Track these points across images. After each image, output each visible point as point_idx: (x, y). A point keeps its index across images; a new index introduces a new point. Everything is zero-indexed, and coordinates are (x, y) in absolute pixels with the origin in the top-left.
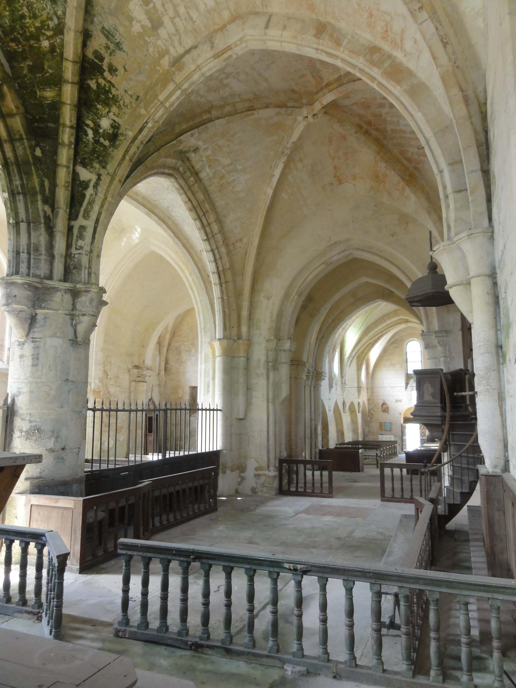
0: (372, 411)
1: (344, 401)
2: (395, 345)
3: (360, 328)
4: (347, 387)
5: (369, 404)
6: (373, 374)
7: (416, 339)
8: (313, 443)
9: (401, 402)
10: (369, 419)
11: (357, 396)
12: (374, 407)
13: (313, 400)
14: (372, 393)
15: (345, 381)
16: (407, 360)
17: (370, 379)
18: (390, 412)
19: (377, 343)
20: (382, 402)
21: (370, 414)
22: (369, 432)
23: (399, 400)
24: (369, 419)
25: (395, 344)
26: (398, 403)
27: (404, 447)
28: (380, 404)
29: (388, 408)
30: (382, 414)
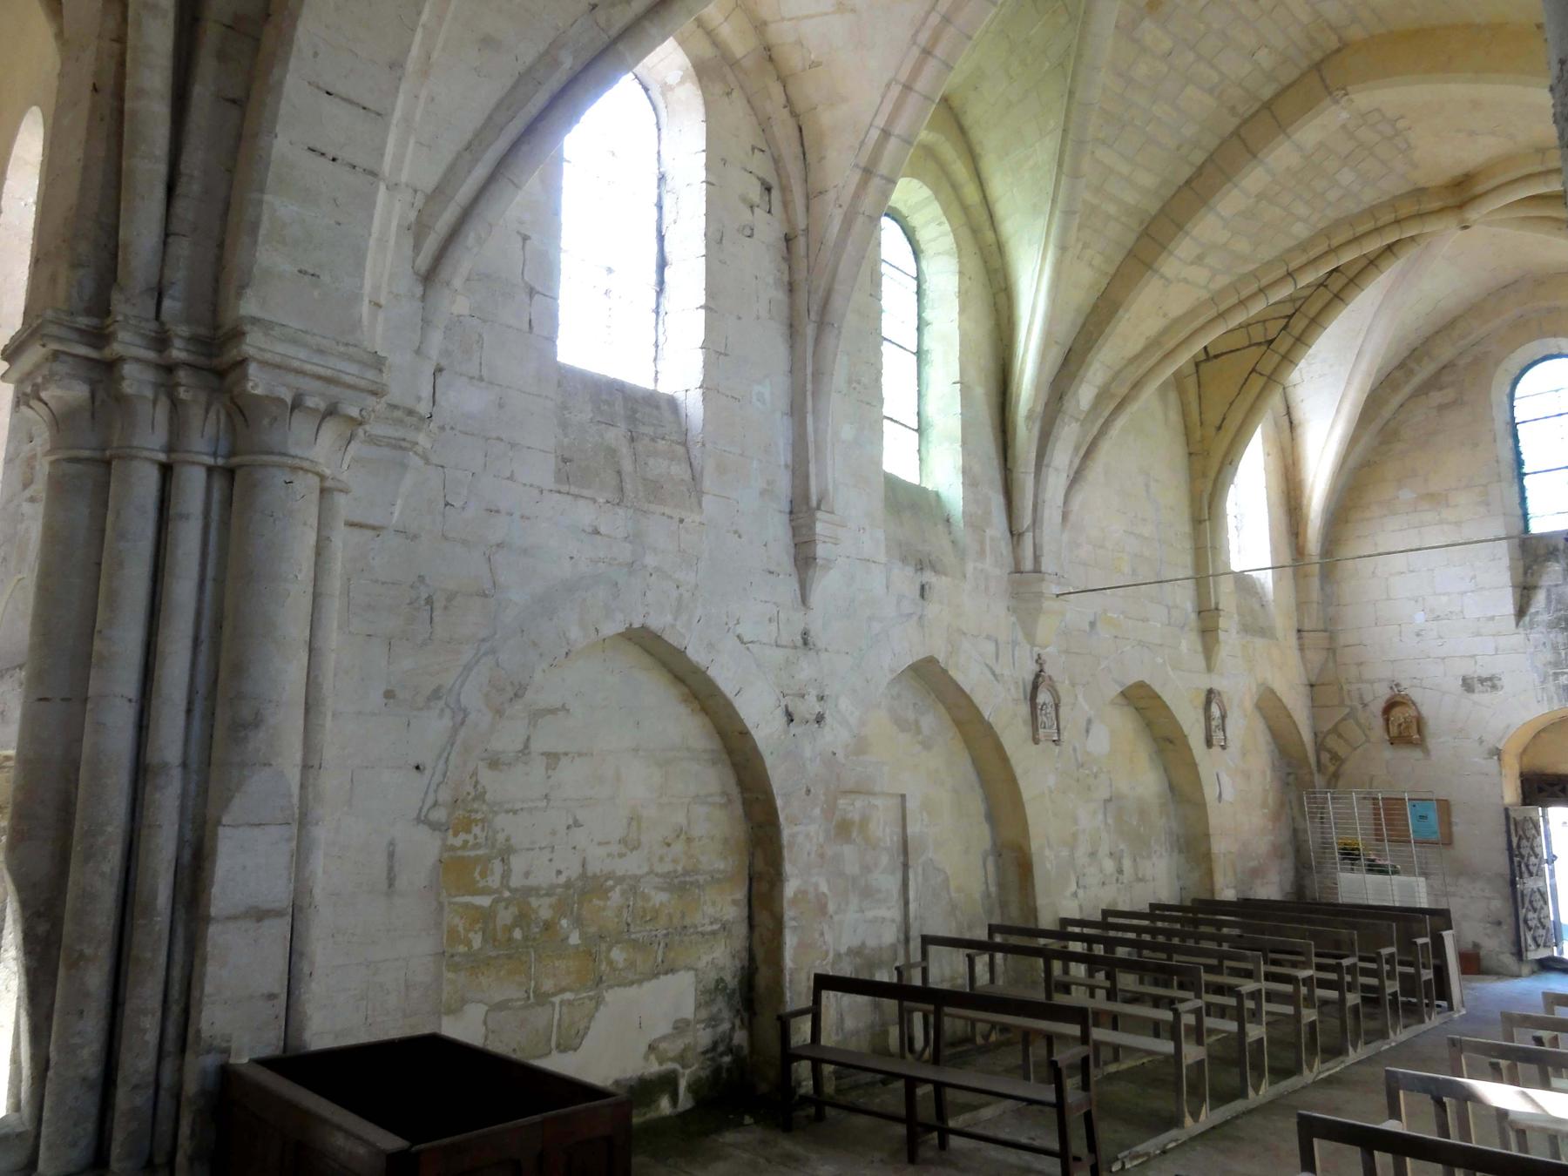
0: (1332, 742)
2: (1437, 397)
8: (146, 995)
9: (1494, 687)
11: (1200, 662)
12: (1344, 719)
13: (183, 590)
14: (1332, 650)
15: (1037, 559)
16: (1520, 463)
17: (1315, 582)
18: (1431, 743)
20: (1383, 694)
21: (1325, 757)
23: (1482, 681)
25: (1441, 389)
26: (1475, 697)
29: (1420, 722)
30: (1388, 753)
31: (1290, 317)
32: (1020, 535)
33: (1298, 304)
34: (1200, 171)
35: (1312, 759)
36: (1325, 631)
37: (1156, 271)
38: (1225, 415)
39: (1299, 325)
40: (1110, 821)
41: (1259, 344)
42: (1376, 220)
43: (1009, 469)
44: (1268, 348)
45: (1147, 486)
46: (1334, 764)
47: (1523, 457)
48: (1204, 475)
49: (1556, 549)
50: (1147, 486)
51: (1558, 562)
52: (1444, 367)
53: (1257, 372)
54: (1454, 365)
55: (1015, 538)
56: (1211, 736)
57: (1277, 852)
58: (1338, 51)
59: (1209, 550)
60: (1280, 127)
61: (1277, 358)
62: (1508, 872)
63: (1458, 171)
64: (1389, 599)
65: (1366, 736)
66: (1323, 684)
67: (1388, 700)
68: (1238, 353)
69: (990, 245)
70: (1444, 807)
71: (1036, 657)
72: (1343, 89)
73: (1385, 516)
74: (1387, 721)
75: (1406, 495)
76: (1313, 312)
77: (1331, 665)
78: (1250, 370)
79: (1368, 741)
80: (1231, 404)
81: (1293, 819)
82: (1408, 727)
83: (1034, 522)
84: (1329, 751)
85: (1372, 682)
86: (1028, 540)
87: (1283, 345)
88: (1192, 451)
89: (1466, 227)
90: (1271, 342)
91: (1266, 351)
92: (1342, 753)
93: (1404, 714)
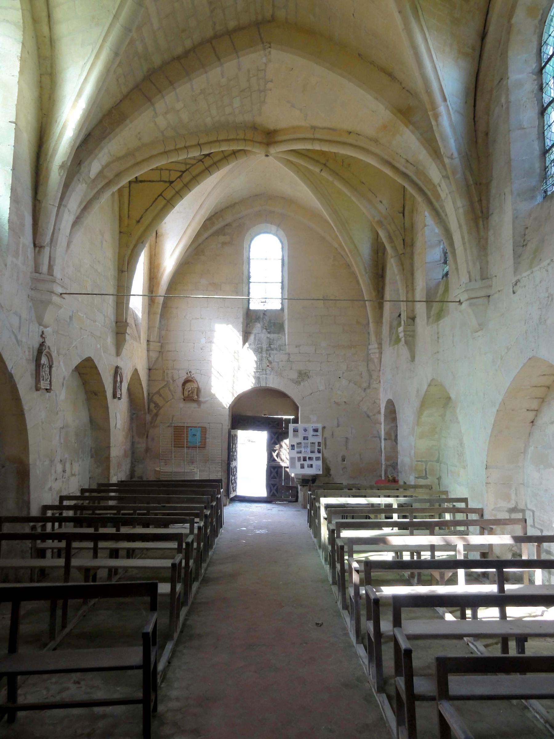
0: (156, 398)
1: (42, 345)
2: (222, 239)
3: (116, 17)
4: (60, 290)
5: (150, 379)
6: (165, 305)
7: (274, 228)
10: (148, 418)
12: (163, 387)
15: (51, 267)
16: (249, 277)
18: (201, 399)
19: (182, 197)
20: (184, 377)
21: (152, 406)
22: (147, 450)
24: (148, 418)
25: (224, 235)
27: (231, 486)
28: (182, 381)
29: (198, 390)
30: (182, 405)
31: (184, 172)
32: (41, 247)
33: (188, 166)
34: (186, 53)
35: (146, 407)
36: (159, 342)
37: (153, 104)
38: (142, 215)
39: (187, 177)
40: (62, 441)
41: (165, 182)
42: (238, 135)
43: (39, 201)
44: (170, 185)
45: (102, 243)
46: (156, 409)
47: (251, 274)
48: (127, 246)
49: (259, 317)
50: (102, 243)
51: (259, 323)
52: (227, 225)
53: (162, 196)
54: (231, 226)
55: (37, 249)
56: (116, 392)
57: (125, 455)
58: (269, 22)
59: (126, 288)
60: (235, 49)
61: (173, 192)
62: (227, 459)
63: (271, 127)
64: (190, 330)
65: (173, 395)
66: (155, 369)
67: (186, 379)
68: (154, 183)
69: (45, 37)
70: (204, 430)
71: (41, 333)
72: (270, 43)
73: (193, 290)
74: (184, 389)
75: (204, 282)
76: (194, 173)
77: (160, 359)
78: (159, 194)
79: (173, 398)
80: (147, 210)
81: (133, 437)
82: (192, 392)
83: (52, 240)
84: (155, 403)
85: (178, 370)
86: (47, 250)
87: (178, 185)
88: (122, 231)
89: (267, 156)
90: (171, 182)
91: (168, 186)
92: (160, 404)
93: (191, 386)
